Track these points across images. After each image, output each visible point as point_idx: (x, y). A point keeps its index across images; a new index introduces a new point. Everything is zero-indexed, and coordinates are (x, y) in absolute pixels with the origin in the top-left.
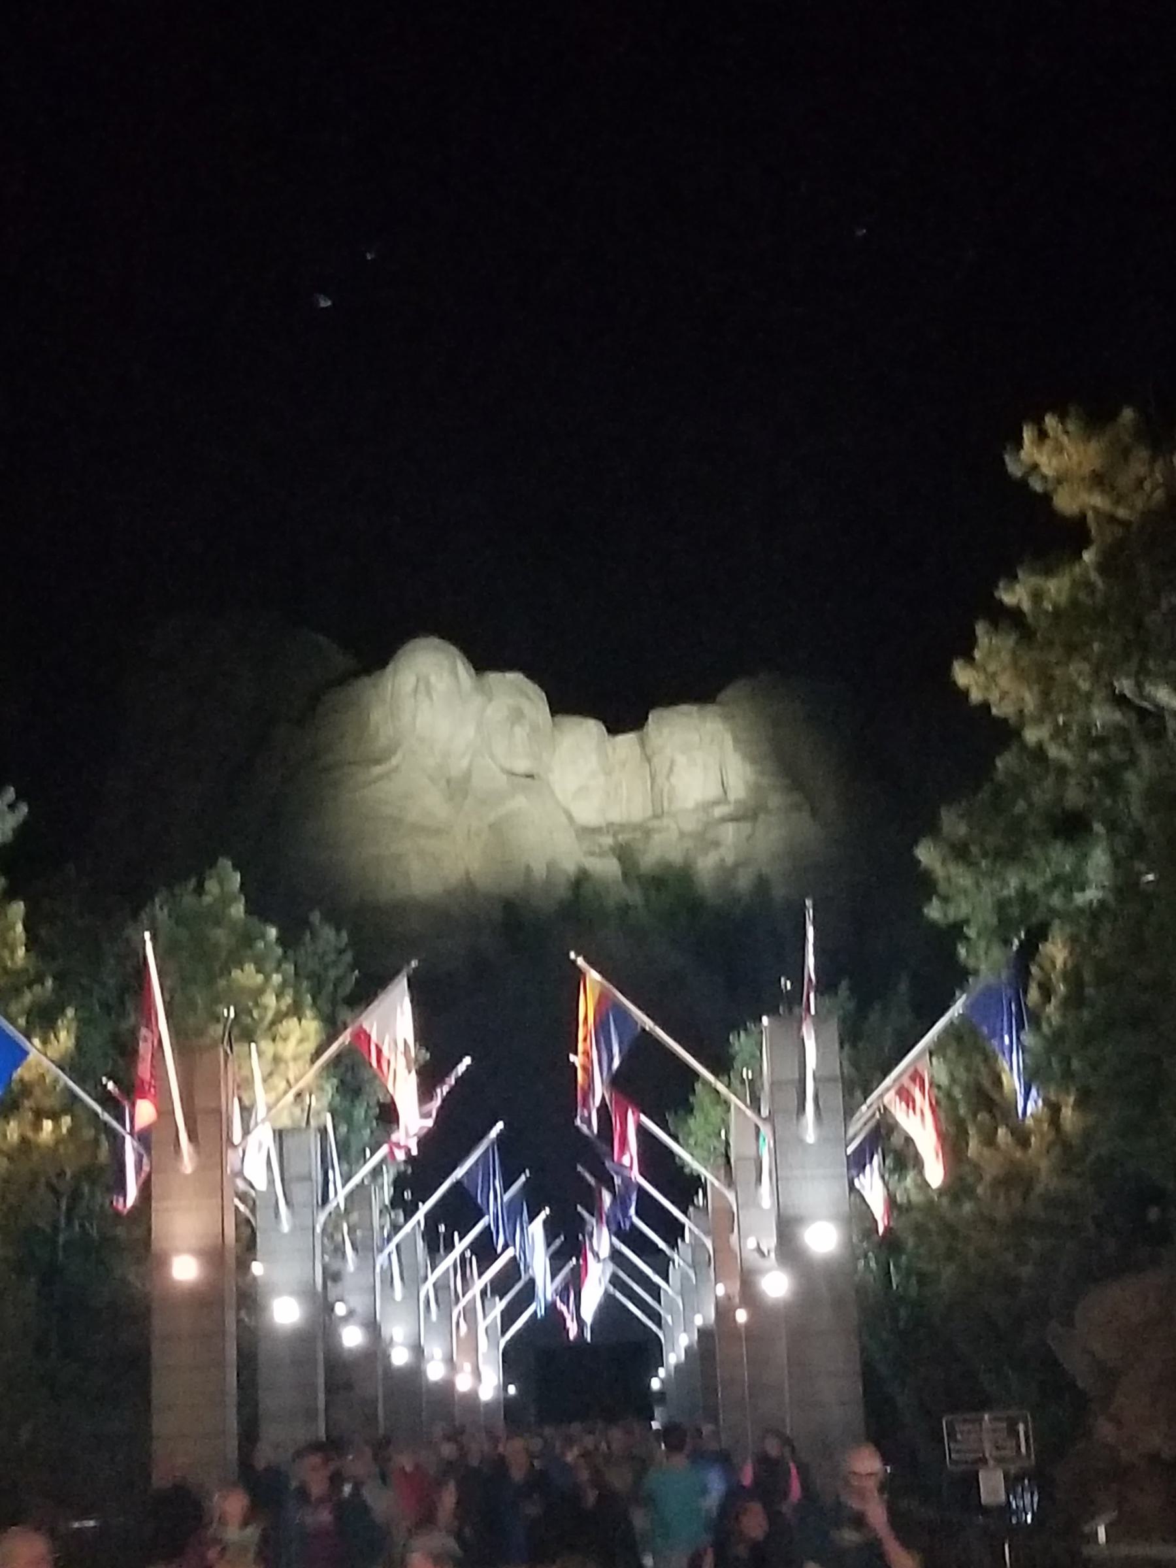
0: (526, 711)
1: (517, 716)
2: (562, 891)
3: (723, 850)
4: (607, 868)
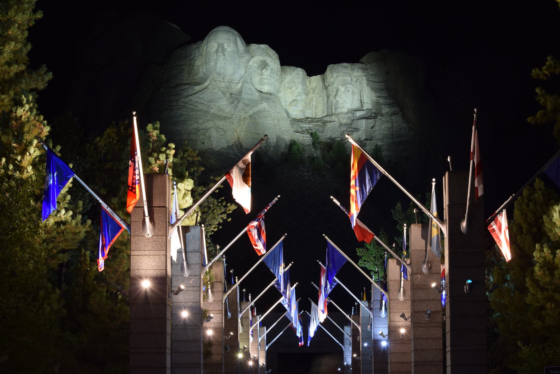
1: (264, 65)
2: (283, 149)
3: (360, 132)
4: (306, 139)
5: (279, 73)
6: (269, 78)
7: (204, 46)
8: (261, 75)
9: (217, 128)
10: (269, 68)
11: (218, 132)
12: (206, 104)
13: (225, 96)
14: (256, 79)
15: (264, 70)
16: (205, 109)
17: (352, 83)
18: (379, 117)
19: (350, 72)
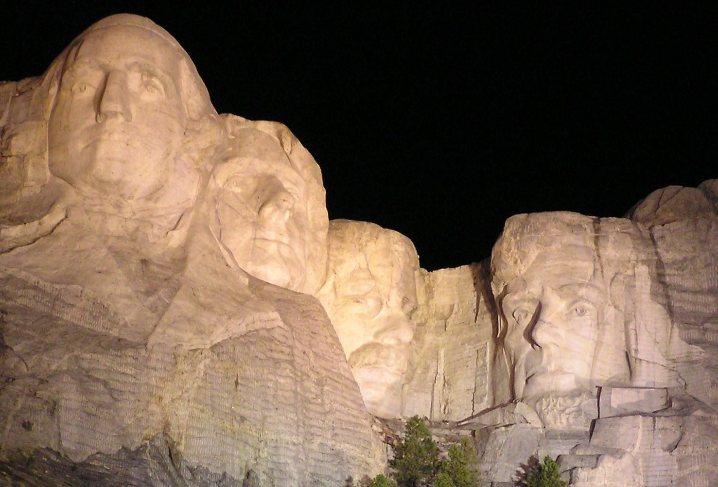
0: (286, 185)
1: (268, 191)
5: (322, 235)
6: (285, 240)
8: (258, 225)
9: (85, 378)
14: (239, 240)
15: (268, 210)
16: (41, 308)
18: (699, 413)
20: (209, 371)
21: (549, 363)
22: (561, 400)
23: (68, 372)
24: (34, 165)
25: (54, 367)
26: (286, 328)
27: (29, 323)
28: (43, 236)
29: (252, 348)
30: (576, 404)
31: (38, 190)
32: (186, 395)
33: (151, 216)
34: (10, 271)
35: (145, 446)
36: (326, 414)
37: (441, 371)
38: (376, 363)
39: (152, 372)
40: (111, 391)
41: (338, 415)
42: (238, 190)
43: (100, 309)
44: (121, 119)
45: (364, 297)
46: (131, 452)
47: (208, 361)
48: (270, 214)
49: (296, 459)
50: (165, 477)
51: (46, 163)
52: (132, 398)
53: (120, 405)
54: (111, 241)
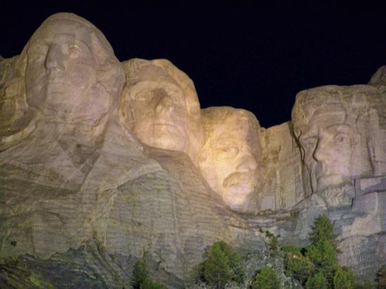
0: (170, 93)
5: (197, 117)
7: (23, 58)
8: (155, 116)
9: (46, 214)
10: (168, 101)
11: (47, 221)
12: (26, 168)
13: (65, 149)
15: (159, 108)
17: (348, 122)
19: (342, 101)
20: (117, 201)
21: (326, 170)
22: (335, 190)
23: (37, 211)
24: (19, 102)
25: (28, 210)
26: (165, 171)
27: (15, 188)
28: (25, 139)
29: (143, 184)
30: (343, 190)
31: (22, 114)
32: (104, 216)
33: (83, 120)
34: (5, 162)
35: (84, 246)
36: (193, 214)
37: (278, 182)
38: (238, 183)
39: (84, 206)
40: (61, 219)
41: (199, 215)
42: (144, 99)
43: (54, 175)
44: (58, 70)
45: (228, 148)
46: (75, 250)
47: (115, 195)
48: (161, 110)
49: (175, 242)
50: (96, 261)
51: (25, 99)
52: (74, 221)
53: (67, 225)
54: (60, 137)
